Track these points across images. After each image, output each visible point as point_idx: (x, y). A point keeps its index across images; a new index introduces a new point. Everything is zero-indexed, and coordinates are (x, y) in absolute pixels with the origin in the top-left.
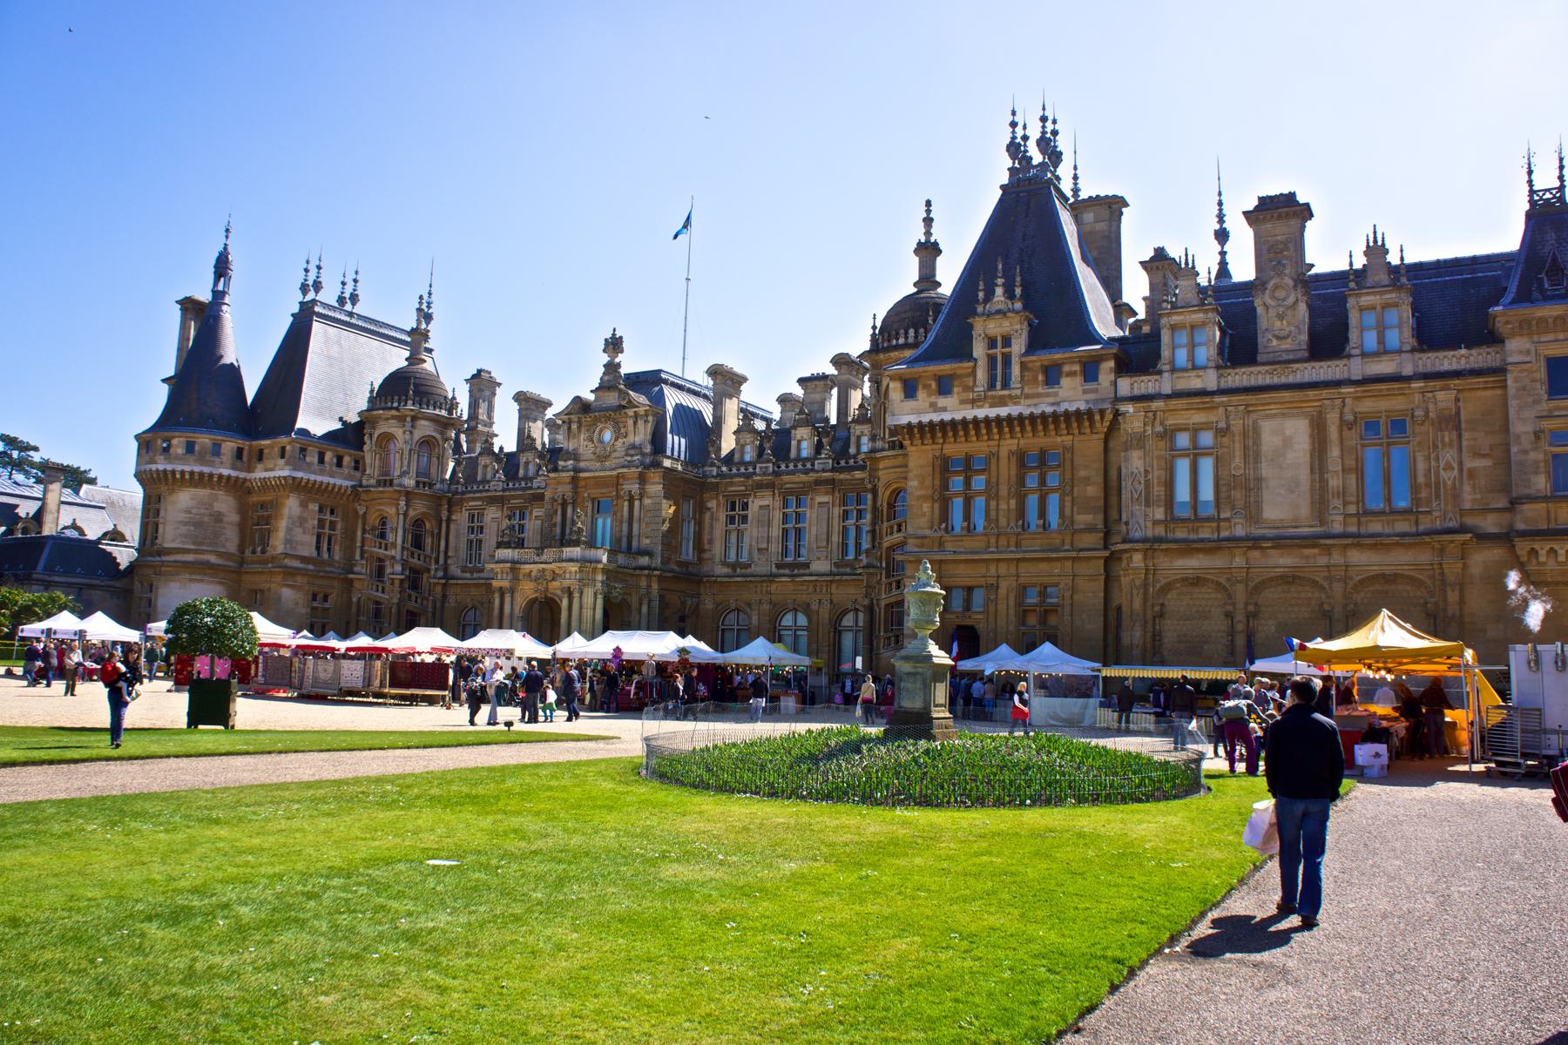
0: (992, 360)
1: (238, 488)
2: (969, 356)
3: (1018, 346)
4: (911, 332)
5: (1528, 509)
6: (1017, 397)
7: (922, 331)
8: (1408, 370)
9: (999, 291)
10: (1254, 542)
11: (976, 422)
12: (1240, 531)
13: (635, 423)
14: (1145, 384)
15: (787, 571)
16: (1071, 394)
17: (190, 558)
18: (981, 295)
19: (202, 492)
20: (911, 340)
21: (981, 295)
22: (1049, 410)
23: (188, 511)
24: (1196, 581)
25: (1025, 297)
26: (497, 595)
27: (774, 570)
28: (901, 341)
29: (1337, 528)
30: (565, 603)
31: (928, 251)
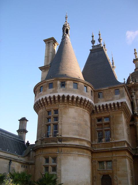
17: (77, 143)
19: (80, 110)
23: (74, 118)
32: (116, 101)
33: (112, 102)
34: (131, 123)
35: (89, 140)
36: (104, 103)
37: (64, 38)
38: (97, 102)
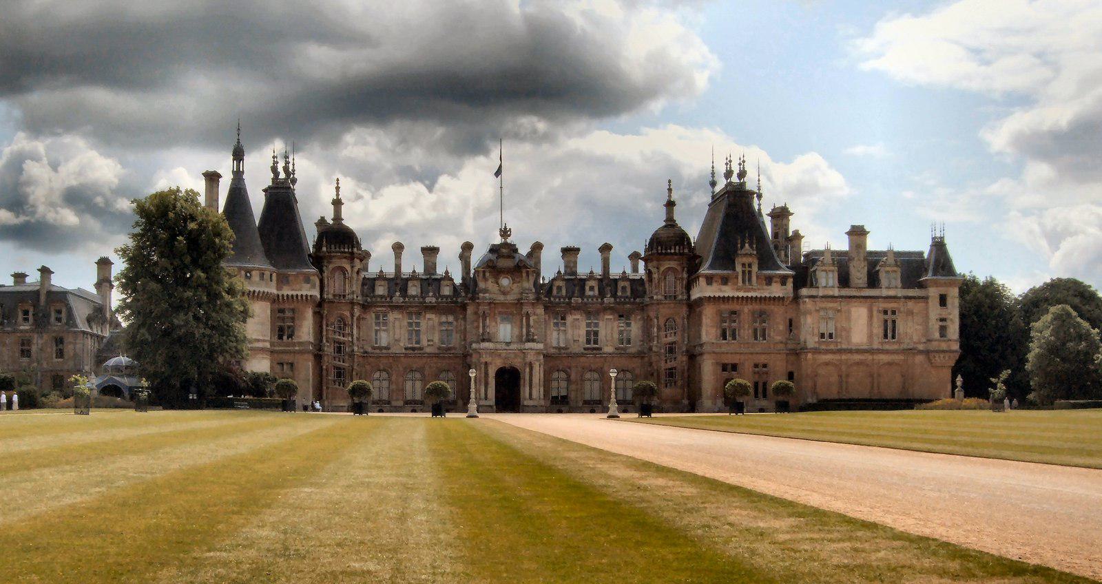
0: (744, 272)
1: (274, 300)
2: (734, 269)
3: (755, 268)
4: (677, 247)
5: (935, 343)
6: (755, 289)
7: (682, 247)
8: (900, 295)
9: (747, 245)
10: (850, 351)
11: (738, 298)
12: (844, 347)
13: (528, 276)
14: (813, 292)
15: (590, 352)
16: (776, 290)
17: (260, 345)
18: (739, 245)
20: (677, 251)
21: (739, 245)
22: (768, 295)
24: (827, 364)
25: (757, 249)
26: (483, 366)
27: (583, 351)
28: (673, 251)
29: (876, 346)
30: (528, 370)
31: (670, 205)
32: (304, 293)
33: (299, 293)
34: (317, 310)
35: (269, 339)
36: (290, 293)
37: (238, 175)
38: (281, 290)
